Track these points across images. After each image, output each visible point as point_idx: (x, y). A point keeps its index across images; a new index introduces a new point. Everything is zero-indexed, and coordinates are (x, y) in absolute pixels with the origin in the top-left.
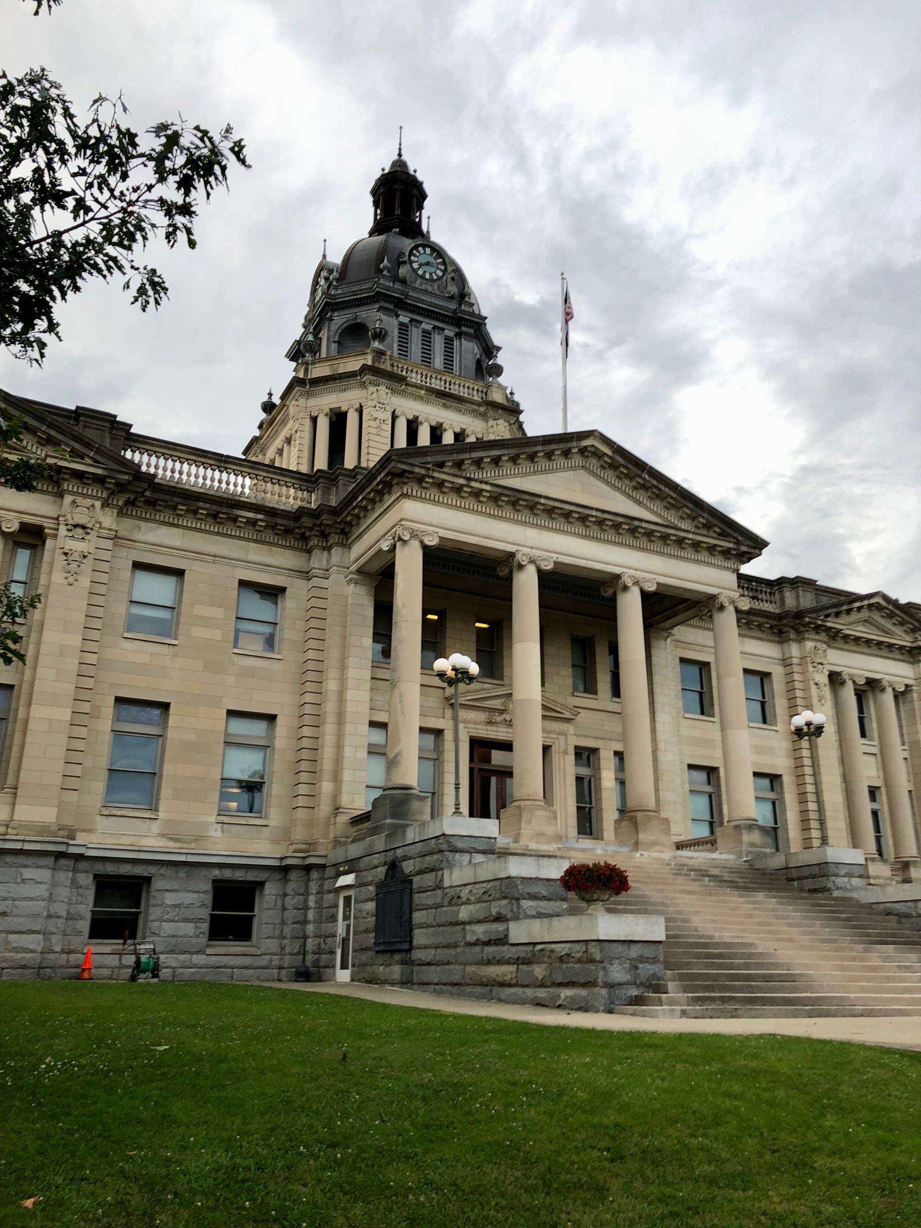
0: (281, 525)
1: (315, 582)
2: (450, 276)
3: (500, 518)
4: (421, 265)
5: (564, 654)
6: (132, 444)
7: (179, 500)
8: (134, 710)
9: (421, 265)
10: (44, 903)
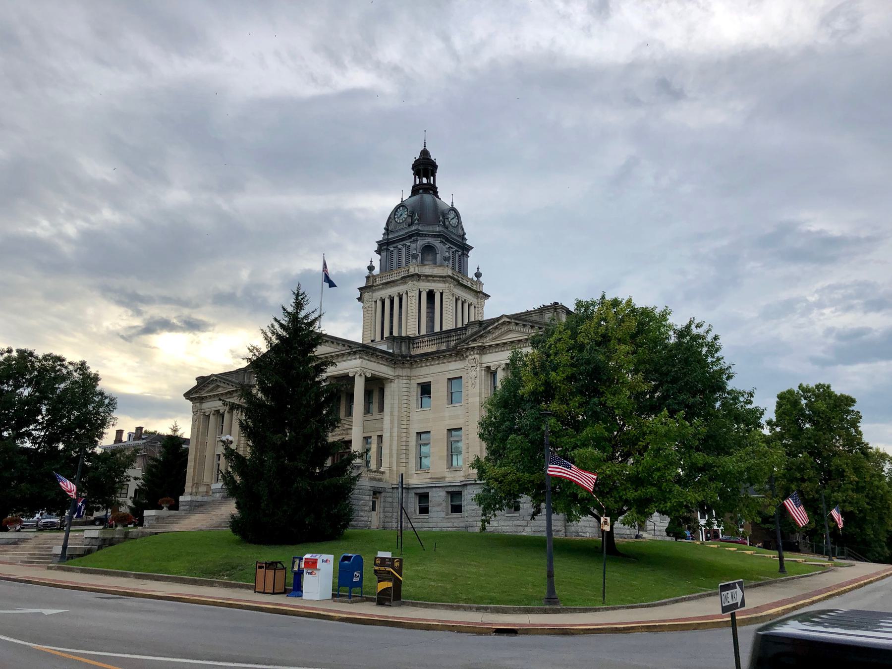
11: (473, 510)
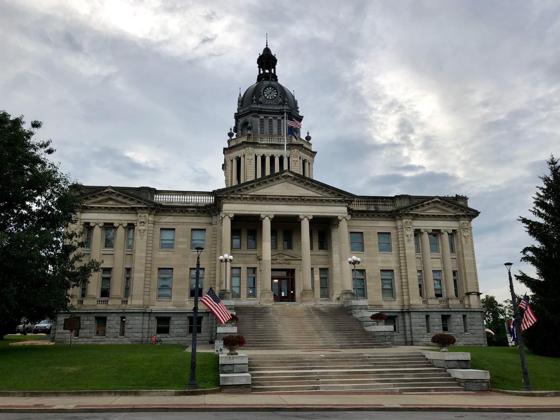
0: (202, 211)
1: (214, 226)
2: (279, 96)
3: (256, 204)
4: (267, 95)
5: (286, 243)
6: (158, 193)
7: (171, 209)
8: (164, 271)
9: (267, 95)
10: (141, 325)
11: (418, 330)
